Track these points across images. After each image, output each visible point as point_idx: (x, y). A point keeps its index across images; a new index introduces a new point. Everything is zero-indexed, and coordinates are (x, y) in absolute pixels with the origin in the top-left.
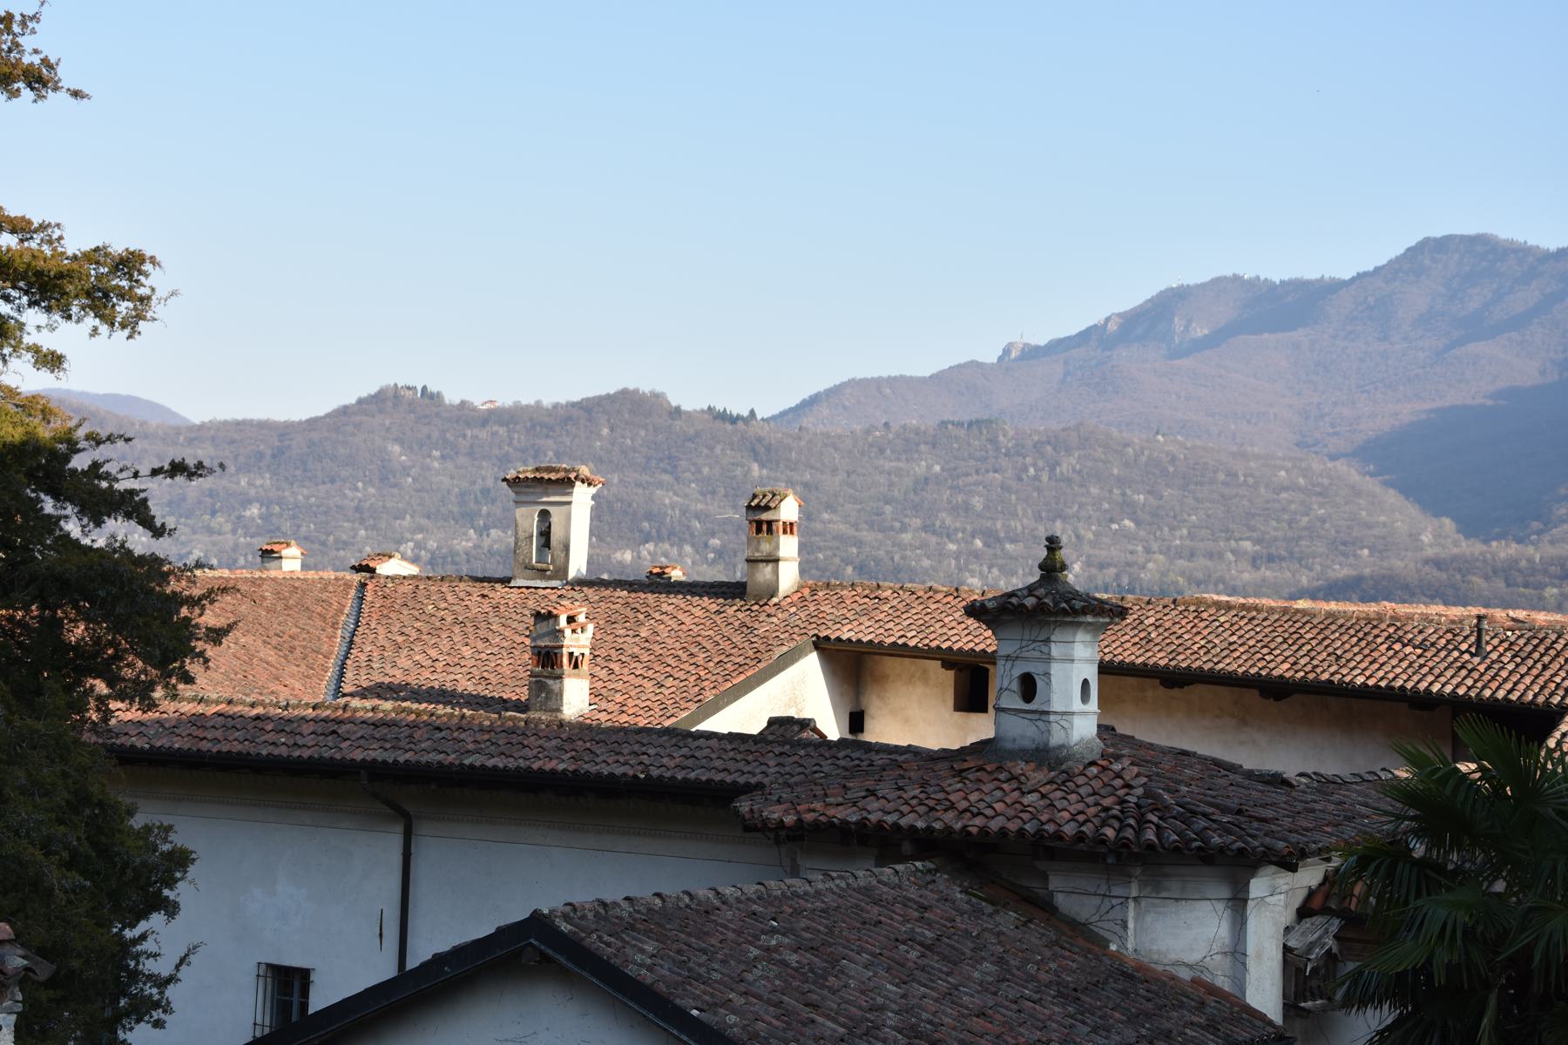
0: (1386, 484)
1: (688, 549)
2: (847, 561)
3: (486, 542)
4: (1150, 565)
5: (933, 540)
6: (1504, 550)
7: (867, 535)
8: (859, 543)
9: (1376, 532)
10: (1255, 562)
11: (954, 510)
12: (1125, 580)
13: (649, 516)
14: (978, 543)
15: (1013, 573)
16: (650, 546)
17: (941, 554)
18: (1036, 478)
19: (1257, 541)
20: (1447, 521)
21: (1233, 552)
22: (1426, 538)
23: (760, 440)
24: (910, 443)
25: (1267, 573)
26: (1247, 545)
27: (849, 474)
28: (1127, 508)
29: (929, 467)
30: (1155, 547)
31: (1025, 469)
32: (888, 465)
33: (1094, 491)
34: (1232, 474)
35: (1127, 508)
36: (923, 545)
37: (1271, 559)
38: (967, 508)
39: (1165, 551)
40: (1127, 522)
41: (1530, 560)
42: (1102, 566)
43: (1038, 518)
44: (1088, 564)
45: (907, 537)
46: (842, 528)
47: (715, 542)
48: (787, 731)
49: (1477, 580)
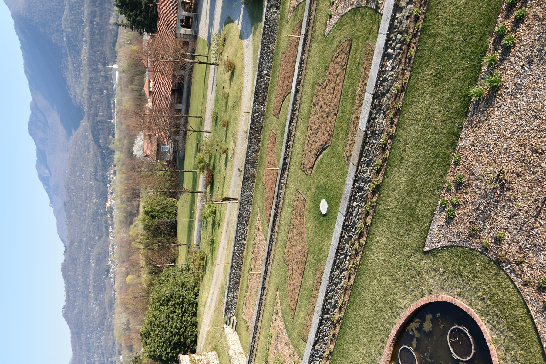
1: (91, 254)
2: (92, 224)
3: (92, 291)
5: (87, 209)
6: (86, 108)
7: (87, 221)
8: (88, 223)
10: (89, 152)
11: (81, 206)
12: (93, 174)
13: (85, 262)
14: (87, 201)
15: (93, 194)
16: (91, 261)
17: (90, 207)
18: (75, 193)
19: (85, 153)
22: (84, 124)
23: (70, 244)
24: (69, 217)
25: (91, 150)
27: (75, 227)
28: (80, 175)
29: (74, 212)
30: (87, 170)
31: (73, 195)
32: (74, 220)
33: (77, 182)
34: (73, 158)
35: (80, 175)
36: (88, 211)
37: (89, 150)
38: (81, 204)
40: (83, 175)
42: (91, 178)
43: (82, 191)
44: (90, 181)
45: (87, 214)
46: (86, 226)
47: (89, 249)
49: (92, 112)
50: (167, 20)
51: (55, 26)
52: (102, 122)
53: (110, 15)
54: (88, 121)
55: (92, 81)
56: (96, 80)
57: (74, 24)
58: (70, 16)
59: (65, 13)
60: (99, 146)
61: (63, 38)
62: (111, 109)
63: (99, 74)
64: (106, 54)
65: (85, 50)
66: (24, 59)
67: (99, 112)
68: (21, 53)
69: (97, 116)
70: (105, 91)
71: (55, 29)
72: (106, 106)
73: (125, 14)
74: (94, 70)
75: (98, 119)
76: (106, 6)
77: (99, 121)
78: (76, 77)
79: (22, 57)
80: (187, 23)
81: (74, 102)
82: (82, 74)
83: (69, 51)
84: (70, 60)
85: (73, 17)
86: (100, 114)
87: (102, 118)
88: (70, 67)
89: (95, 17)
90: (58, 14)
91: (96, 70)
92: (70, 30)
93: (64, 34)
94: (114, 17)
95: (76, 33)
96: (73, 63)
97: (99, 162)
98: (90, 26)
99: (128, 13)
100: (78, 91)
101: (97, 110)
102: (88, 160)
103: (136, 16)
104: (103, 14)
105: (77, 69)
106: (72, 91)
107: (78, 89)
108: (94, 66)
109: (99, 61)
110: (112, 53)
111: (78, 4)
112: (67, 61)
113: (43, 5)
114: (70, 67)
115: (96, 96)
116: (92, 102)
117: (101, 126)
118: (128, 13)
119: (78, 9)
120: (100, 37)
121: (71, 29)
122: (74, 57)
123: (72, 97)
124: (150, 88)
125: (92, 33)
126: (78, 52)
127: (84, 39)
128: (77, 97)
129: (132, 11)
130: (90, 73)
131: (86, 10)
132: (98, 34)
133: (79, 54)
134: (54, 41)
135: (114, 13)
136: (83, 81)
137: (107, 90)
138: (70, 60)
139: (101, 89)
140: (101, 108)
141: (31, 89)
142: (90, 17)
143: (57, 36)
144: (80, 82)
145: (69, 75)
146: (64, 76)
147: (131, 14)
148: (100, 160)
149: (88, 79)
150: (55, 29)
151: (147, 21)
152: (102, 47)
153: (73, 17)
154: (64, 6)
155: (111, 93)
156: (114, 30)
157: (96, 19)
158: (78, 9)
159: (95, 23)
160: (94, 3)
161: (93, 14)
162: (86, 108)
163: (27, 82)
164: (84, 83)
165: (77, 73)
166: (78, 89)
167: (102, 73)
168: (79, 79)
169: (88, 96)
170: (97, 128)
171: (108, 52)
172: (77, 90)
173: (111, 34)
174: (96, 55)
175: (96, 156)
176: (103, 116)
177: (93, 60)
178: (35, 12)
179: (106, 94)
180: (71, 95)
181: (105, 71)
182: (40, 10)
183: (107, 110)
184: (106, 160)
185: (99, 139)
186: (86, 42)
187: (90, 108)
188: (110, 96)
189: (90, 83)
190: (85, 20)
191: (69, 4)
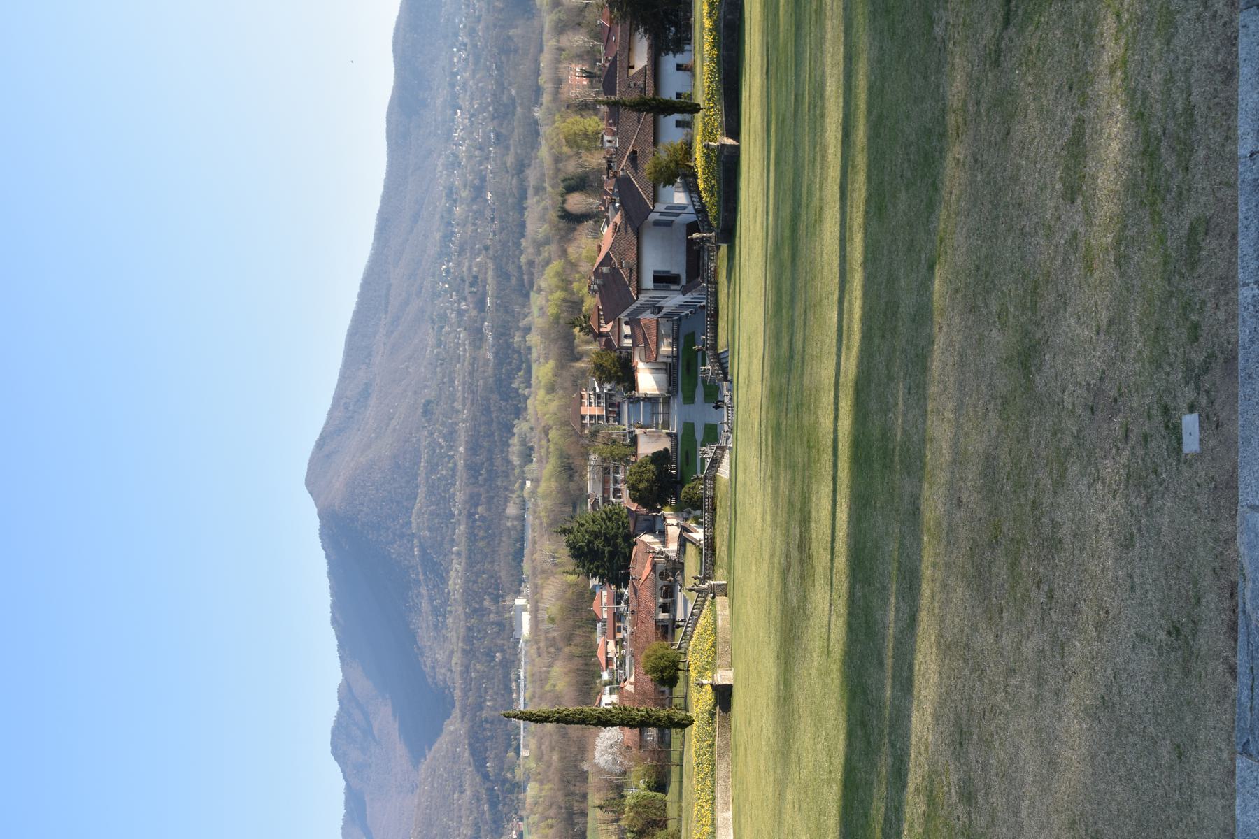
0: (430, 749)
4: (465, 832)
6: (458, 694)
9: (449, 747)
10: (462, 792)
19: (454, 793)
20: (445, 723)
21: (458, 800)
22: (452, 728)
25: (467, 787)
26: (456, 796)
30: (457, 832)
39: (458, 828)
41: (461, 684)
48: (610, 552)
50: (647, 607)
51: (398, 527)
52: (492, 723)
53: (506, 500)
54: (462, 721)
55: (471, 634)
56: (479, 631)
57: (436, 521)
58: (428, 506)
59: (418, 501)
60: (486, 776)
61: (412, 549)
62: (510, 692)
63: (485, 618)
64: (500, 577)
65: (456, 570)
66: (332, 596)
67: (485, 701)
68: (326, 583)
69: (482, 709)
70: (498, 655)
71: (398, 532)
72: (501, 686)
73: (583, 567)
74: (475, 611)
75: (484, 714)
76: (499, 483)
77: (486, 721)
78: (436, 627)
79: (328, 591)
80: (665, 608)
81: (430, 680)
82: (450, 620)
83: (425, 574)
84: (424, 591)
85: (433, 507)
86: (488, 704)
87: (493, 713)
88: (425, 607)
89: (477, 505)
90: (405, 504)
91: (479, 612)
92: (427, 533)
93: (416, 541)
94: (514, 503)
95: (439, 538)
96: (431, 599)
97: (483, 813)
98: (467, 524)
99: (587, 565)
100: (441, 656)
101: (481, 697)
102: (460, 810)
103: (598, 568)
104: (493, 498)
105: (440, 612)
106: (427, 657)
107: (441, 652)
108: (476, 602)
109: (485, 593)
110: (512, 575)
111: (444, 482)
112: (419, 594)
113: (377, 490)
114: (425, 607)
115: (479, 667)
116: (471, 679)
117: (490, 731)
118: (587, 565)
119: (444, 491)
120: (488, 543)
121: (430, 529)
122: (434, 587)
123: (428, 670)
124: (607, 653)
125: (472, 537)
126: (442, 576)
127: (454, 549)
128: (437, 670)
129: (591, 562)
130: (468, 617)
131: (460, 494)
132: (483, 539)
133: (443, 579)
134: (394, 556)
135: (514, 496)
136: (453, 636)
137: (503, 651)
138: (424, 591)
139: (490, 649)
140: (490, 692)
141: (341, 658)
142: (467, 506)
143: (400, 546)
144: (445, 638)
145: (423, 623)
146: (412, 627)
147: (591, 566)
148: (486, 807)
149: (462, 631)
150: (398, 532)
151: (612, 574)
152: (492, 562)
153: (433, 507)
154: (417, 486)
155: (512, 658)
156: (514, 528)
157: (480, 509)
158: (444, 491)
159: (477, 517)
160: (477, 478)
161: (474, 500)
162: (458, 694)
163: (335, 642)
164: (454, 640)
165: (440, 618)
166: (441, 652)
167: (492, 616)
168: (444, 631)
169: (462, 666)
170: (481, 736)
171: (503, 574)
172: (437, 656)
173: (510, 536)
174: (480, 580)
175: (478, 800)
176: (494, 708)
177: (474, 591)
178: (362, 504)
179: (501, 661)
180: (426, 666)
181: (497, 613)
182: (371, 500)
183: (503, 695)
184: (500, 807)
185: (485, 760)
186: (459, 554)
187: (465, 692)
188: (510, 663)
189: (468, 639)
190: (456, 512)
191: (427, 482)
